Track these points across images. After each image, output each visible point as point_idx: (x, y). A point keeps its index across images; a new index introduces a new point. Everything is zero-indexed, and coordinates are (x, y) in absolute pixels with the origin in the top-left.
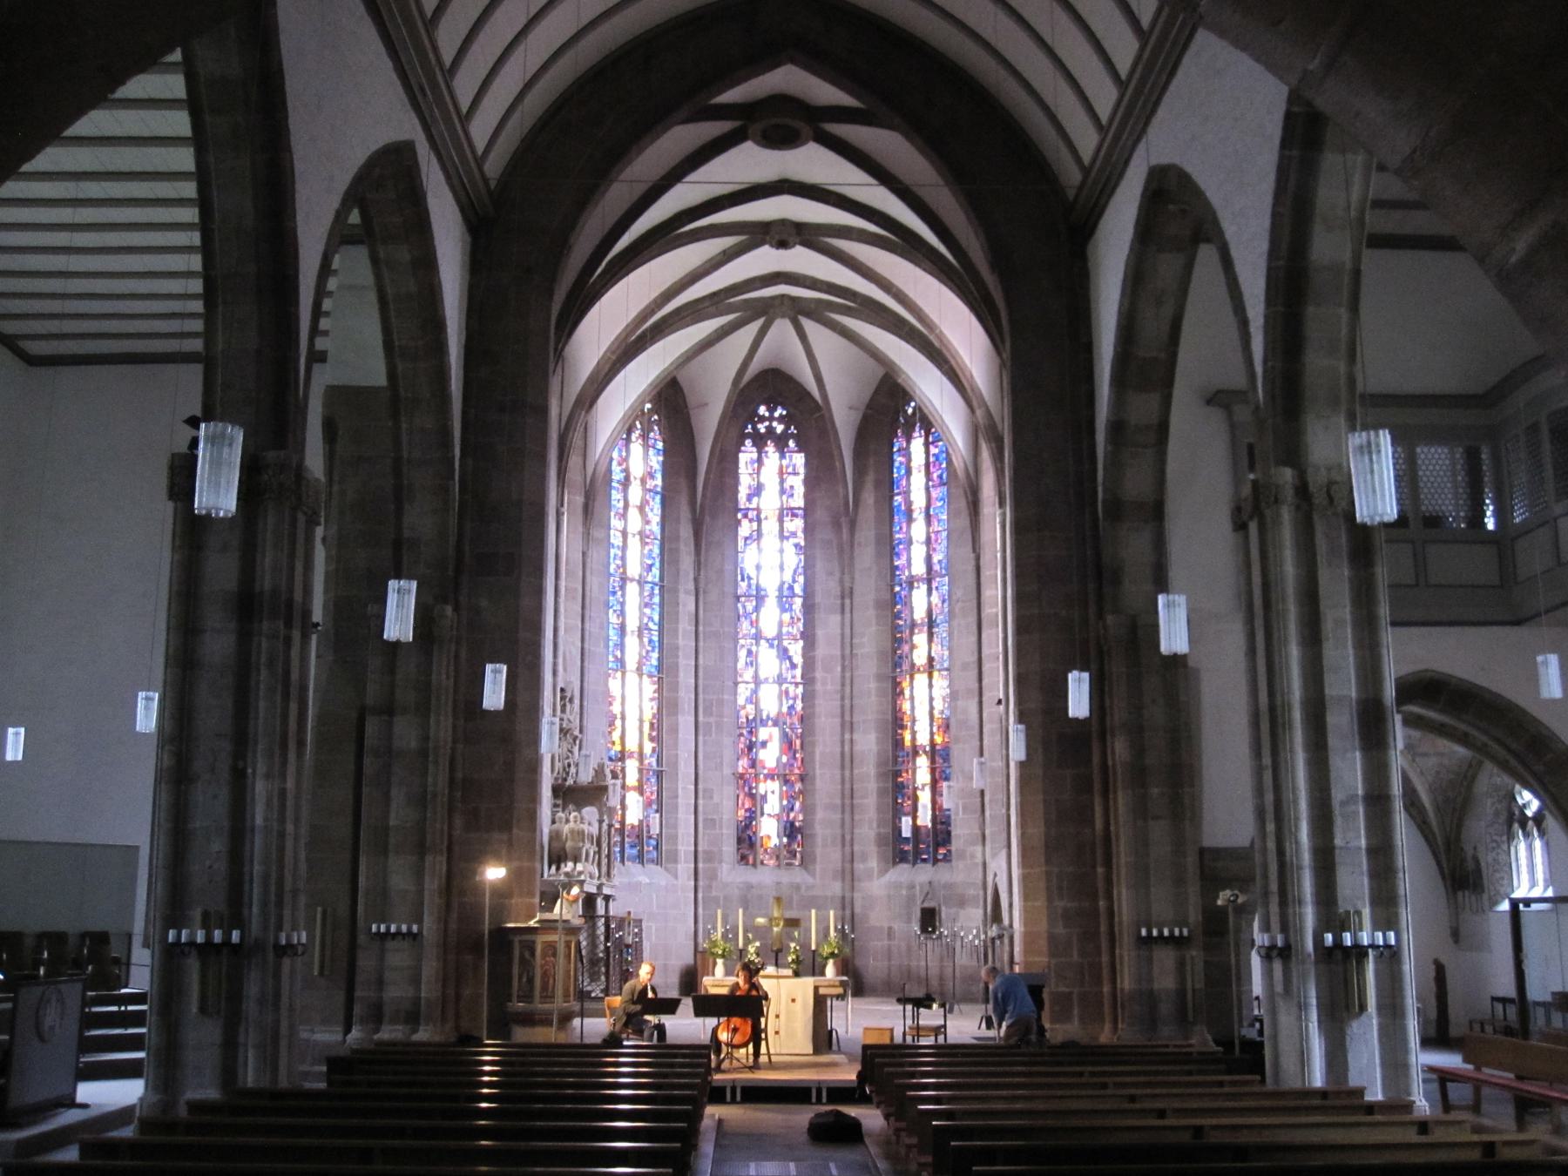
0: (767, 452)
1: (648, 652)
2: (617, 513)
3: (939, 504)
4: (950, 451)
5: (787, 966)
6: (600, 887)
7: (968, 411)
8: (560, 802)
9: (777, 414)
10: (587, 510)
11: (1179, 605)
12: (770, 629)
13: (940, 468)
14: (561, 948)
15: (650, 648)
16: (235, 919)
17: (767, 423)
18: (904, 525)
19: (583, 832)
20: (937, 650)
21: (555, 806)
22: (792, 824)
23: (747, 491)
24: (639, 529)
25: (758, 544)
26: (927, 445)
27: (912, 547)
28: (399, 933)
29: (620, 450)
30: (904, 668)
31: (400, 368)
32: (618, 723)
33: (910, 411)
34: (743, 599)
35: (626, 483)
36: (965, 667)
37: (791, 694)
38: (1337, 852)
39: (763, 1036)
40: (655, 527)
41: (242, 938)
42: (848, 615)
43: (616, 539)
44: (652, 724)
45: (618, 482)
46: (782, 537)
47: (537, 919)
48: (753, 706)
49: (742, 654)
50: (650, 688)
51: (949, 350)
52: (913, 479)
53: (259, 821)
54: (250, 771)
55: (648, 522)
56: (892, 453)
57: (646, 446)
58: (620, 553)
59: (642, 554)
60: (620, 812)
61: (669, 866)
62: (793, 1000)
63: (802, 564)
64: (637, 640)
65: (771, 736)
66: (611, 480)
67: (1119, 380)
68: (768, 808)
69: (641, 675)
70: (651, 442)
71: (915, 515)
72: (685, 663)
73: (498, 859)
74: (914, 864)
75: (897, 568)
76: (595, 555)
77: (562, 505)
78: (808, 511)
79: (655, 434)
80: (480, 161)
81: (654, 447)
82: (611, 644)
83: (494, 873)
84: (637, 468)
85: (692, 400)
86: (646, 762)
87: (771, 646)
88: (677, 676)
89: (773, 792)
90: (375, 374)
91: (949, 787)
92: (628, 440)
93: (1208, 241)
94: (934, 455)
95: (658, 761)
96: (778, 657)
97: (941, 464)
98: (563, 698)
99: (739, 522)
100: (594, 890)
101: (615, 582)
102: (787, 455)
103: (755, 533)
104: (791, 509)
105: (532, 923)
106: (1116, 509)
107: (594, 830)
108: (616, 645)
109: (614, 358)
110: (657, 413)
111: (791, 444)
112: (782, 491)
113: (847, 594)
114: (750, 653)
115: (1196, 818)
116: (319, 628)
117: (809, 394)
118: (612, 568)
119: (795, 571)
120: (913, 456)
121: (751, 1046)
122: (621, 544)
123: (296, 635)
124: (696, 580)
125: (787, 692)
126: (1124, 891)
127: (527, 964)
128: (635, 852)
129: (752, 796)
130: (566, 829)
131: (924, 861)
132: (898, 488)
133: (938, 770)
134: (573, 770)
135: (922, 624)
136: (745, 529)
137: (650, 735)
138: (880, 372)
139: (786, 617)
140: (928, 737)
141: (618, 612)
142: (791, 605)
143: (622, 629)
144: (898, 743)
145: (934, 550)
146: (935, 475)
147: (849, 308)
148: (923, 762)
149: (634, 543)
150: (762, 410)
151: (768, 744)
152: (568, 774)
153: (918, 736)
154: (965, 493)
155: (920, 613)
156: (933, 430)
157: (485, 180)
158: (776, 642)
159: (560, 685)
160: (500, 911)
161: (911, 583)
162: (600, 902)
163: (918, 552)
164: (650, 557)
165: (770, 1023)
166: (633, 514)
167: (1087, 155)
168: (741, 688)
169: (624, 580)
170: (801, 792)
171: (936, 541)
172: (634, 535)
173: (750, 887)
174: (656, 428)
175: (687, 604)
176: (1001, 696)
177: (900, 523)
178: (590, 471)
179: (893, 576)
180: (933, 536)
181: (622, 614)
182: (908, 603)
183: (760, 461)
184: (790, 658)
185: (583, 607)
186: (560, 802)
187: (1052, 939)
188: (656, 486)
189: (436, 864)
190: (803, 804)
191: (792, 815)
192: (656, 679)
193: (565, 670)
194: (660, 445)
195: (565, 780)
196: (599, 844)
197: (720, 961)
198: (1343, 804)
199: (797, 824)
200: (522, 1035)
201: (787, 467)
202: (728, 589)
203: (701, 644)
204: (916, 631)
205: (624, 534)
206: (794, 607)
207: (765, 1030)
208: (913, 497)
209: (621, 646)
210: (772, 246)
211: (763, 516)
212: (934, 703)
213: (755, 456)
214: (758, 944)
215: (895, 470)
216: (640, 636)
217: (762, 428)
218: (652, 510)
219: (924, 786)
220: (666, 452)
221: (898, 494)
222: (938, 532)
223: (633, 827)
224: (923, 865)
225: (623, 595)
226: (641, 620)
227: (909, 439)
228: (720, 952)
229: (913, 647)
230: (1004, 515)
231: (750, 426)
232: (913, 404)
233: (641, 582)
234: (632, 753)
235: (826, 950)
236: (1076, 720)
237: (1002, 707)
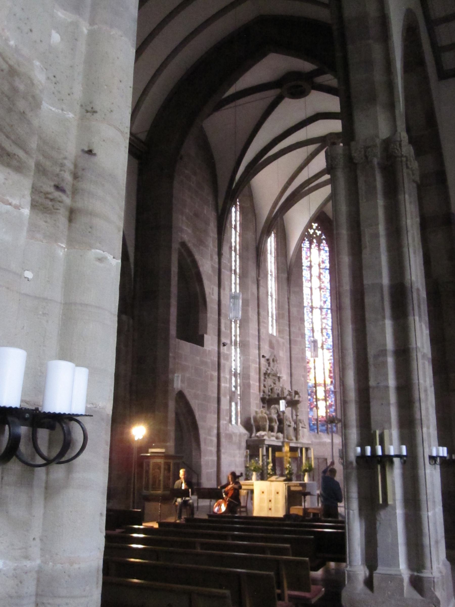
1: (326, 339)
2: (306, 280)
15: (327, 337)
24: (319, 286)
32: (312, 371)
35: (310, 267)
38: (371, 390)
45: (307, 267)
55: (323, 282)
57: (319, 250)
62: (263, 492)
70: (321, 248)
76: (293, 298)
77: (259, 276)
79: (324, 244)
81: (323, 250)
101: (306, 311)
118: (305, 304)
128: (324, 428)
143: (313, 330)
149: (316, 292)
164: (324, 297)
169: (312, 308)
172: (316, 289)
174: (324, 241)
178: (289, 263)
185: (289, 321)
188: (326, 266)
192: (331, 351)
194: (327, 249)
198: (376, 356)
205: (311, 288)
216: (322, 332)
218: (324, 277)
223: (322, 417)
225: (312, 315)
226: (322, 325)
233: (321, 308)
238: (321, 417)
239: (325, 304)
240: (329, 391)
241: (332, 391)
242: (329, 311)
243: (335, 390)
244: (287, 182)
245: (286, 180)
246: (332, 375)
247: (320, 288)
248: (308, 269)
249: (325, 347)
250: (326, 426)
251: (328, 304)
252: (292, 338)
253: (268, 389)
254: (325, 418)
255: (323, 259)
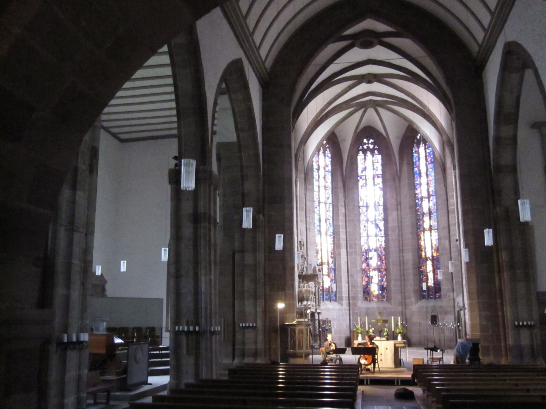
0: (367, 155)
1: (329, 227)
2: (316, 180)
3: (431, 170)
4: (434, 151)
5: (384, 336)
6: (316, 310)
7: (440, 136)
8: (301, 280)
9: (370, 142)
10: (305, 179)
11: (526, 204)
12: (371, 218)
13: (431, 157)
14: (305, 331)
15: (330, 226)
16: (197, 323)
17: (367, 145)
18: (419, 178)
19: (310, 290)
20: (434, 223)
21: (300, 282)
22: (383, 286)
23: (361, 170)
24: (324, 185)
25: (366, 188)
26: (425, 149)
27: (422, 186)
28: (249, 327)
29: (316, 158)
30: (421, 229)
31: (241, 135)
32: (320, 252)
33: (418, 137)
34: (361, 208)
35: (318, 169)
36: (444, 228)
37: (380, 240)
39: (377, 361)
40: (329, 184)
41: (199, 328)
42: (399, 212)
43: (316, 188)
44: (331, 253)
45: (316, 169)
46: (374, 185)
47: (296, 321)
48: (367, 245)
49: (362, 227)
50: (330, 240)
51: (431, 114)
52: (421, 161)
53: (203, 290)
54: (199, 273)
55: (327, 182)
56: (412, 153)
57: (325, 156)
58: (317, 194)
59: (325, 194)
60: (322, 283)
61: (340, 302)
62: (387, 349)
63: (382, 194)
64: (325, 224)
65: (374, 256)
66: (313, 168)
67: (497, 122)
68: (373, 281)
69: (327, 236)
70: (326, 154)
71: (422, 175)
72: (342, 231)
73: (282, 300)
74: (428, 299)
75: (416, 194)
77: (297, 178)
78: (383, 176)
79: (328, 152)
80: (264, 63)
81: (327, 156)
82: (316, 225)
83: (281, 306)
84: (322, 165)
85: (340, 139)
86: (330, 266)
87: (372, 223)
88: (339, 235)
89: (375, 275)
90: (233, 137)
91: (440, 272)
92: (318, 154)
93: (529, 67)
94: (428, 153)
95: (334, 265)
96: (375, 227)
97: (431, 156)
98: (300, 245)
99: (358, 181)
100: (314, 311)
101: (316, 204)
102: (375, 156)
103: (365, 184)
104: (377, 175)
105: (294, 323)
106: (499, 169)
107: (313, 290)
108: (318, 225)
109: (312, 126)
110: (328, 144)
111: (376, 152)
112: (374, 169)
113: (399, 204)
114: (365, 226)
115: (535, 280)
116: (218, 224)
117: (381, 134)
118: (315, 199)
119: (380, 197)
120: (420, 154)
121: (372, 365)
122: (318, 191)
123: (212, 227)
124: (345, 202)
125: (379, 240)
126: (508, 308)
127: (293, 336)
128: (327, 297)
129: (368, 277)
130: (304, 289)
131: (431, 298)
132: (416, 165)
133: (435, 266)
134: (305, 269)
135: (427, 214)
136: (361, 183)
137: (331, 256)
138: (406, 124)
139: (377, 213)
140: (431, 254)
141: (318, 214)
142: (379, 209)
144: (420, 256)
145: (430, 187)
146: (429, 160)
147: (395, 103)
148: (429, 263)
149: (322, 189)
150: (365, 141)
151: (373, 258)
152: (303, 270)
153: (427, 254)
154: (440, 165)
155: (426, 210)
156: (427, 144)
157: (265, 68)
158: (374, 222)
159: (299, 240)
160: (283, 319)
161: (422, 199)
162: (316, 315)
163: (424, 188)
164: (328, 194)
165: (379, 357)
166: (321, 179)
167: (480, 41)
168: (362, 239)
170: (385, 275)
171: (430, 183)
173: (368, 309)
174: (328, 149)
175: (342, 210)
176: (458, 238)
177: (417, 178)
178: (306, 165)
179: (415, 196)
180: (429, 182)
181: (319, 215)
182: (421, 206)
183: (365, 159)
184: (379, 228)
185: (306, 213)
186: (301, 280)
187: (481, 326)
188: (329, 170)
189: (261, 303)
190: (386, 279)
191: (382, 283)
192: (332, 237)
193: (301, 234)
194: (330, 155)
195: (302, 273)
196: (315, 295)
197: (360, 335)
199: (385, 286)
200: (293, 361)
201: (375, 160)
202: (356, 204)
203: (347, 224)
204: (425, 216)
205: (319, 187)
206: (380, 209)
207: (377, 359)
208: (421, 168)
209: (320, 226)
210: (366, 83)
211: (367, 178)
212: (433, 242)
213: (363, 157)
214: (373, 329)
215: (414, 159)
217: (365, 147)
218: (328, 178)
219: (430, 271)
220: (332, 158)
221: (416, 167)
222: (431, 180)
223: (326, 288)
224: (431, 300)
225: (319, 208)
227: (418, 147)
228: (360, 332)
229: (424, 222)
230: (455, 173)
231: (361, 147)
232: (419, 135)
233: (325, 203)
234: (325, 263)
235: (398, 331)
236: (488, 247)
237: (458, 242)
238: (325, 289)
239: (328, 200)
240: (331, 268)
241: (333, 269)
242: (331, 206)
243: (335, 268)
244: (325, 105)
245: (325, 103)
246: (333, 256)
247: (325, 187)
248: (317, 171)
249: (328, 234)
250: (329, 296)
251: (330, 200)
252: (308, 226)
253: (302, 267)
254: (328, 289)
255: (327, 163)
